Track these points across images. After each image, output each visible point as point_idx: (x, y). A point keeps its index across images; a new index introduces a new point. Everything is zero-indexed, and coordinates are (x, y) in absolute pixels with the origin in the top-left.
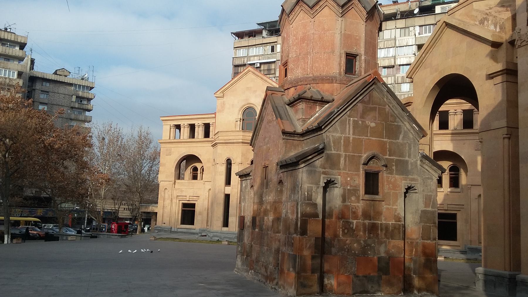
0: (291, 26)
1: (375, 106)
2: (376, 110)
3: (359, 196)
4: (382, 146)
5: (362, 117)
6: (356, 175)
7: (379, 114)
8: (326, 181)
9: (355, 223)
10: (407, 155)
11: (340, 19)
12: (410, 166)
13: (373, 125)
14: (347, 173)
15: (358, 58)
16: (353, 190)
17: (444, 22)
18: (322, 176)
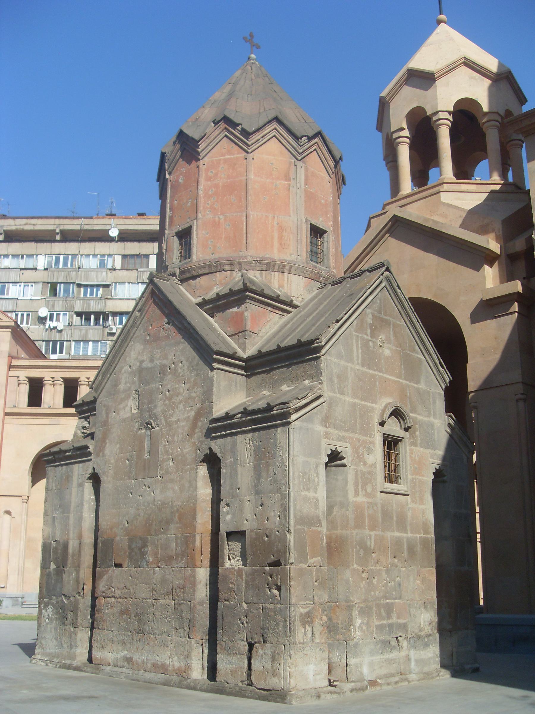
0: (201, 162)
1: (388, 318)
2: (390, 325)
3: (376, 485)
4: (402, 392)
5: (373, 335)
6: (371, 443)
7: (395, 334)
8: (329, 452)
9: (373, 538)
10: (432, 413)
11: (299, 164)
12: (436, 432)
13: (387, 352)
14: (359, 440)
15: (325, 236)
16: (369, 473)
17: (395, 216)
18: (324, 441)
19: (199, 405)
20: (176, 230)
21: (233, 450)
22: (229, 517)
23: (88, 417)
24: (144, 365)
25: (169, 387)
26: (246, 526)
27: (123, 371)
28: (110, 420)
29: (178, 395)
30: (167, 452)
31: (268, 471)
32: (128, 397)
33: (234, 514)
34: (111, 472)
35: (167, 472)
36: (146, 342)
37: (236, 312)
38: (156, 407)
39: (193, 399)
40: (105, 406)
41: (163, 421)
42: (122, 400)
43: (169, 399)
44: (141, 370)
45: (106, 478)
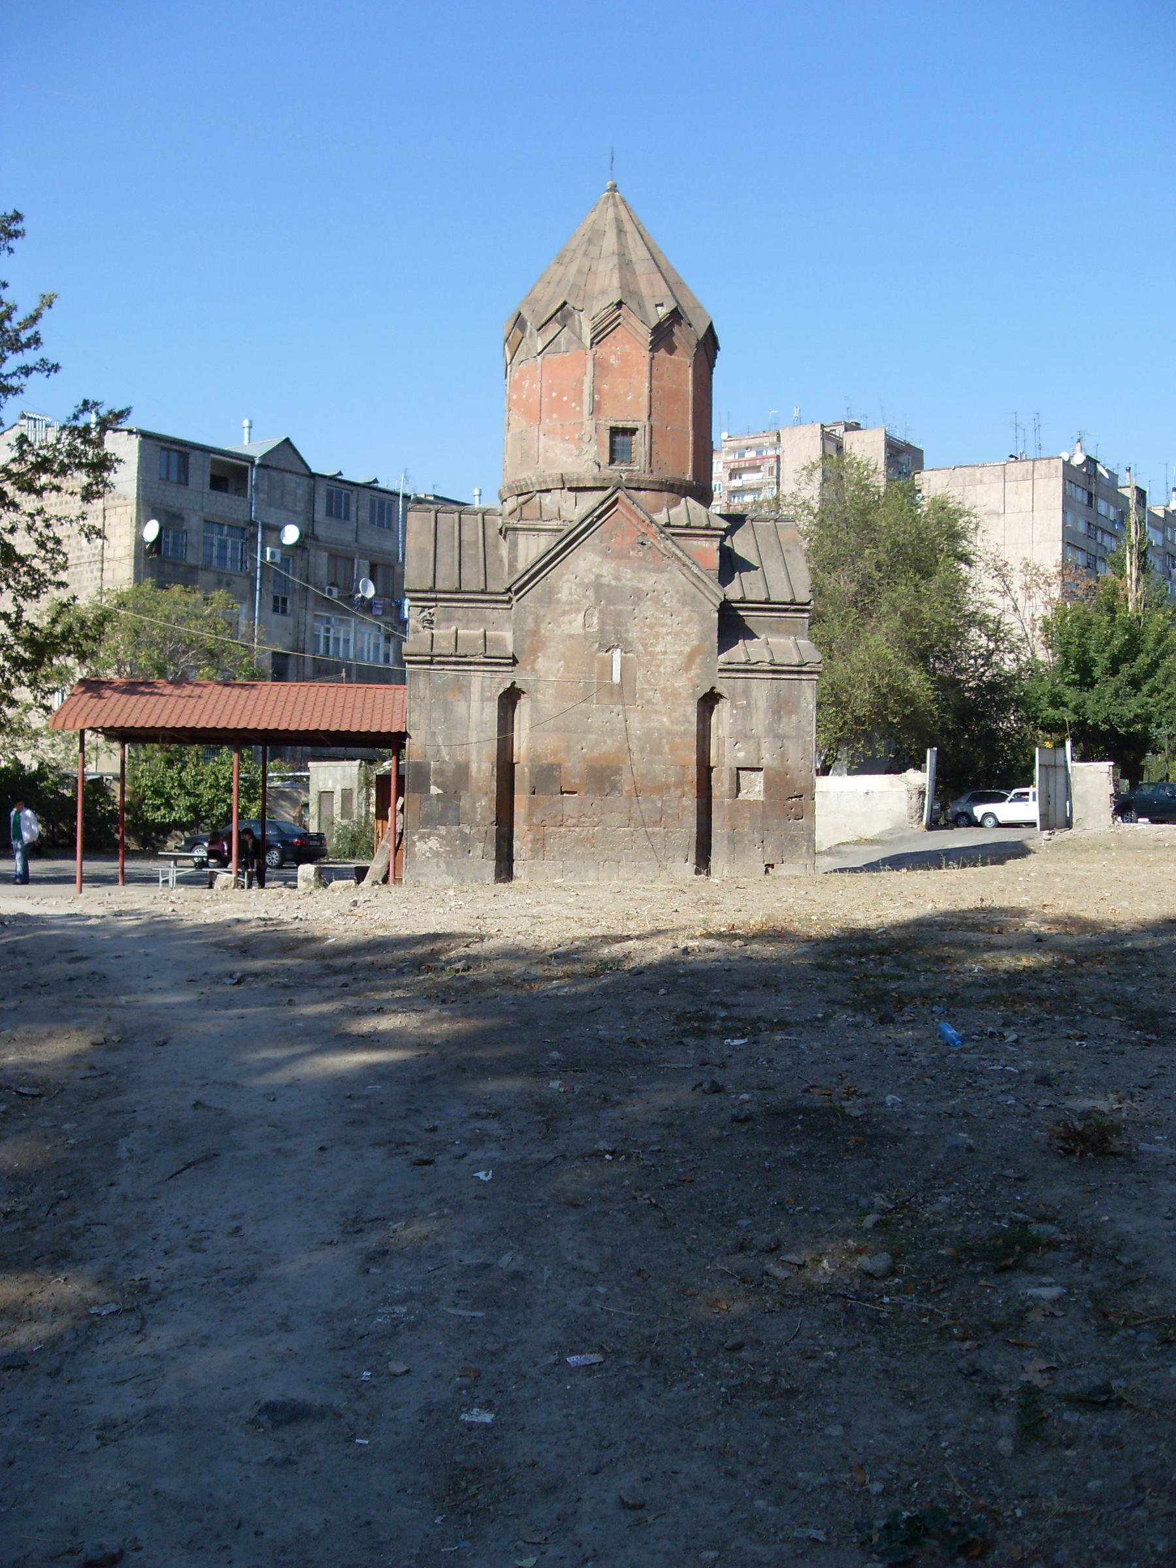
19: (695, 643)
20: (613, 424)
21: (746, 693)
22: (741, 754)
23: (431, 607)
24: (605, 581)
25: (648, 614)
26: (764, 763)
27: (565, 578)
28: (543, 631)
29: (663, 626)
30: (649, 682)
31: (790, 718)
32: (578, 611)
33: (747, 753)
34: (551, 691)
35: (649, 702)
36: (605, 555)
37: (705, 549)
38: (627, 631)
39: (686, 634)
40: (531, 613)
41: (641, 648)
42: (564, 613)
43: (651, 627)
44: (598, 586)
45: (540, 697)
